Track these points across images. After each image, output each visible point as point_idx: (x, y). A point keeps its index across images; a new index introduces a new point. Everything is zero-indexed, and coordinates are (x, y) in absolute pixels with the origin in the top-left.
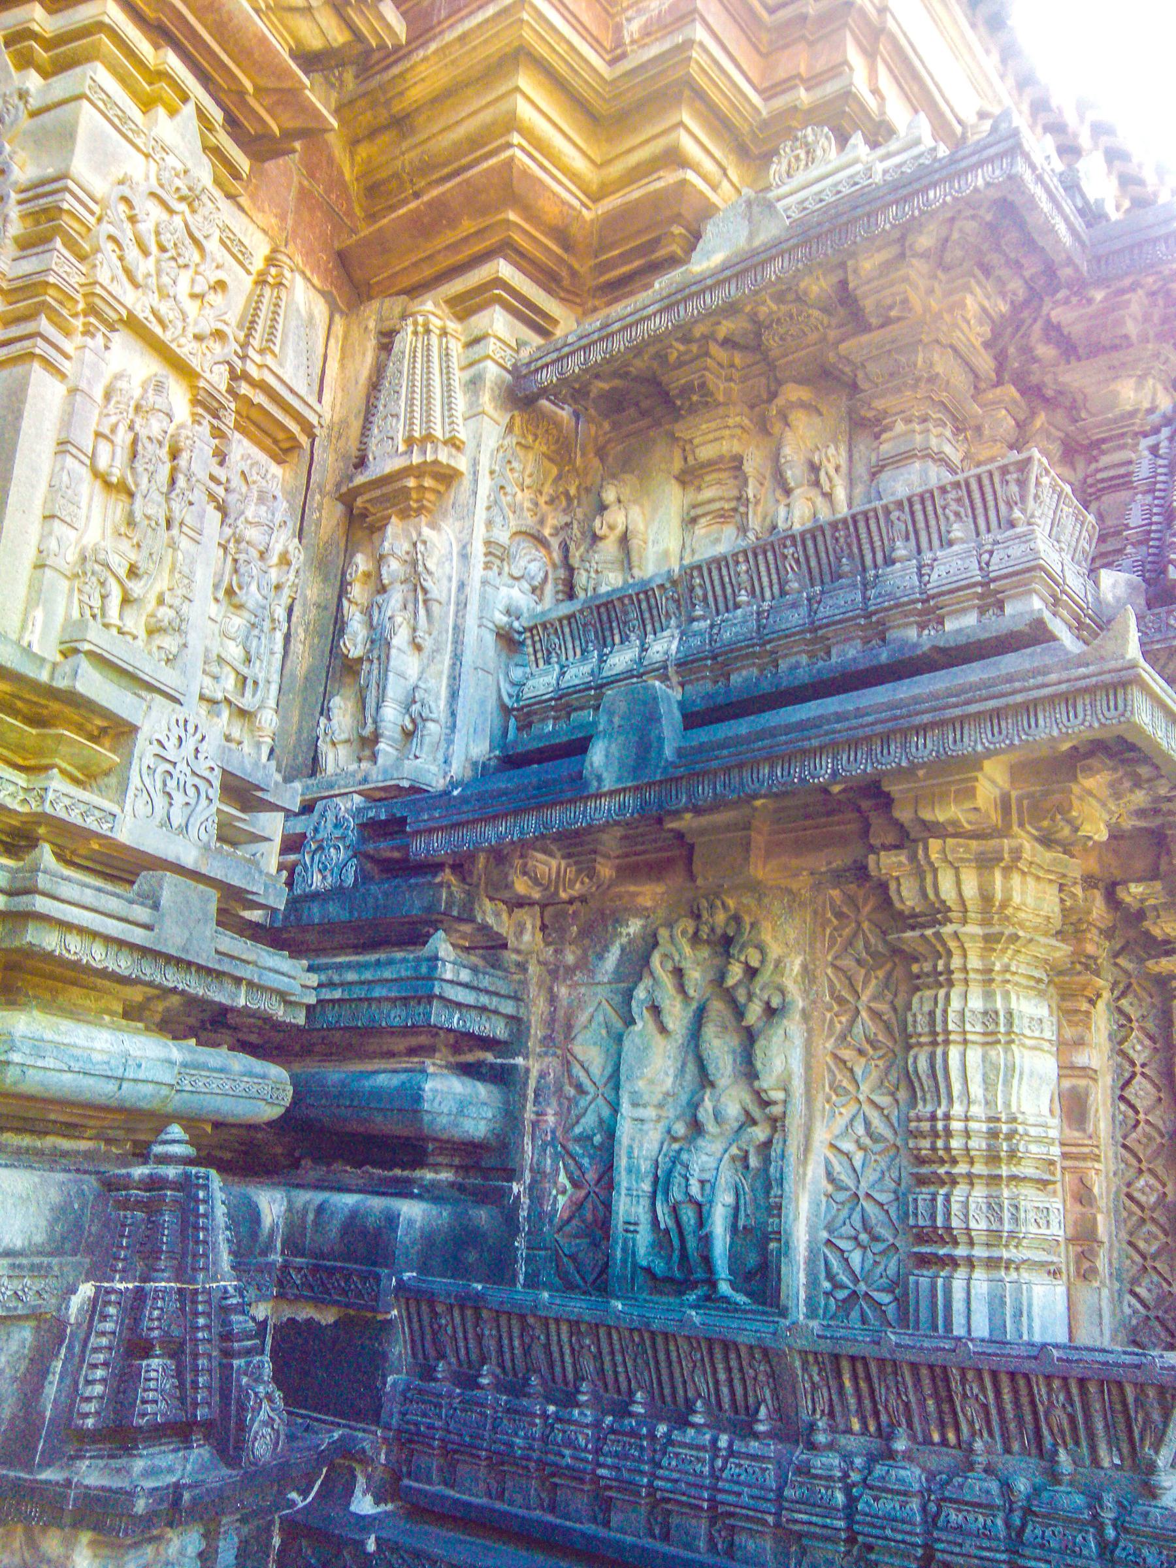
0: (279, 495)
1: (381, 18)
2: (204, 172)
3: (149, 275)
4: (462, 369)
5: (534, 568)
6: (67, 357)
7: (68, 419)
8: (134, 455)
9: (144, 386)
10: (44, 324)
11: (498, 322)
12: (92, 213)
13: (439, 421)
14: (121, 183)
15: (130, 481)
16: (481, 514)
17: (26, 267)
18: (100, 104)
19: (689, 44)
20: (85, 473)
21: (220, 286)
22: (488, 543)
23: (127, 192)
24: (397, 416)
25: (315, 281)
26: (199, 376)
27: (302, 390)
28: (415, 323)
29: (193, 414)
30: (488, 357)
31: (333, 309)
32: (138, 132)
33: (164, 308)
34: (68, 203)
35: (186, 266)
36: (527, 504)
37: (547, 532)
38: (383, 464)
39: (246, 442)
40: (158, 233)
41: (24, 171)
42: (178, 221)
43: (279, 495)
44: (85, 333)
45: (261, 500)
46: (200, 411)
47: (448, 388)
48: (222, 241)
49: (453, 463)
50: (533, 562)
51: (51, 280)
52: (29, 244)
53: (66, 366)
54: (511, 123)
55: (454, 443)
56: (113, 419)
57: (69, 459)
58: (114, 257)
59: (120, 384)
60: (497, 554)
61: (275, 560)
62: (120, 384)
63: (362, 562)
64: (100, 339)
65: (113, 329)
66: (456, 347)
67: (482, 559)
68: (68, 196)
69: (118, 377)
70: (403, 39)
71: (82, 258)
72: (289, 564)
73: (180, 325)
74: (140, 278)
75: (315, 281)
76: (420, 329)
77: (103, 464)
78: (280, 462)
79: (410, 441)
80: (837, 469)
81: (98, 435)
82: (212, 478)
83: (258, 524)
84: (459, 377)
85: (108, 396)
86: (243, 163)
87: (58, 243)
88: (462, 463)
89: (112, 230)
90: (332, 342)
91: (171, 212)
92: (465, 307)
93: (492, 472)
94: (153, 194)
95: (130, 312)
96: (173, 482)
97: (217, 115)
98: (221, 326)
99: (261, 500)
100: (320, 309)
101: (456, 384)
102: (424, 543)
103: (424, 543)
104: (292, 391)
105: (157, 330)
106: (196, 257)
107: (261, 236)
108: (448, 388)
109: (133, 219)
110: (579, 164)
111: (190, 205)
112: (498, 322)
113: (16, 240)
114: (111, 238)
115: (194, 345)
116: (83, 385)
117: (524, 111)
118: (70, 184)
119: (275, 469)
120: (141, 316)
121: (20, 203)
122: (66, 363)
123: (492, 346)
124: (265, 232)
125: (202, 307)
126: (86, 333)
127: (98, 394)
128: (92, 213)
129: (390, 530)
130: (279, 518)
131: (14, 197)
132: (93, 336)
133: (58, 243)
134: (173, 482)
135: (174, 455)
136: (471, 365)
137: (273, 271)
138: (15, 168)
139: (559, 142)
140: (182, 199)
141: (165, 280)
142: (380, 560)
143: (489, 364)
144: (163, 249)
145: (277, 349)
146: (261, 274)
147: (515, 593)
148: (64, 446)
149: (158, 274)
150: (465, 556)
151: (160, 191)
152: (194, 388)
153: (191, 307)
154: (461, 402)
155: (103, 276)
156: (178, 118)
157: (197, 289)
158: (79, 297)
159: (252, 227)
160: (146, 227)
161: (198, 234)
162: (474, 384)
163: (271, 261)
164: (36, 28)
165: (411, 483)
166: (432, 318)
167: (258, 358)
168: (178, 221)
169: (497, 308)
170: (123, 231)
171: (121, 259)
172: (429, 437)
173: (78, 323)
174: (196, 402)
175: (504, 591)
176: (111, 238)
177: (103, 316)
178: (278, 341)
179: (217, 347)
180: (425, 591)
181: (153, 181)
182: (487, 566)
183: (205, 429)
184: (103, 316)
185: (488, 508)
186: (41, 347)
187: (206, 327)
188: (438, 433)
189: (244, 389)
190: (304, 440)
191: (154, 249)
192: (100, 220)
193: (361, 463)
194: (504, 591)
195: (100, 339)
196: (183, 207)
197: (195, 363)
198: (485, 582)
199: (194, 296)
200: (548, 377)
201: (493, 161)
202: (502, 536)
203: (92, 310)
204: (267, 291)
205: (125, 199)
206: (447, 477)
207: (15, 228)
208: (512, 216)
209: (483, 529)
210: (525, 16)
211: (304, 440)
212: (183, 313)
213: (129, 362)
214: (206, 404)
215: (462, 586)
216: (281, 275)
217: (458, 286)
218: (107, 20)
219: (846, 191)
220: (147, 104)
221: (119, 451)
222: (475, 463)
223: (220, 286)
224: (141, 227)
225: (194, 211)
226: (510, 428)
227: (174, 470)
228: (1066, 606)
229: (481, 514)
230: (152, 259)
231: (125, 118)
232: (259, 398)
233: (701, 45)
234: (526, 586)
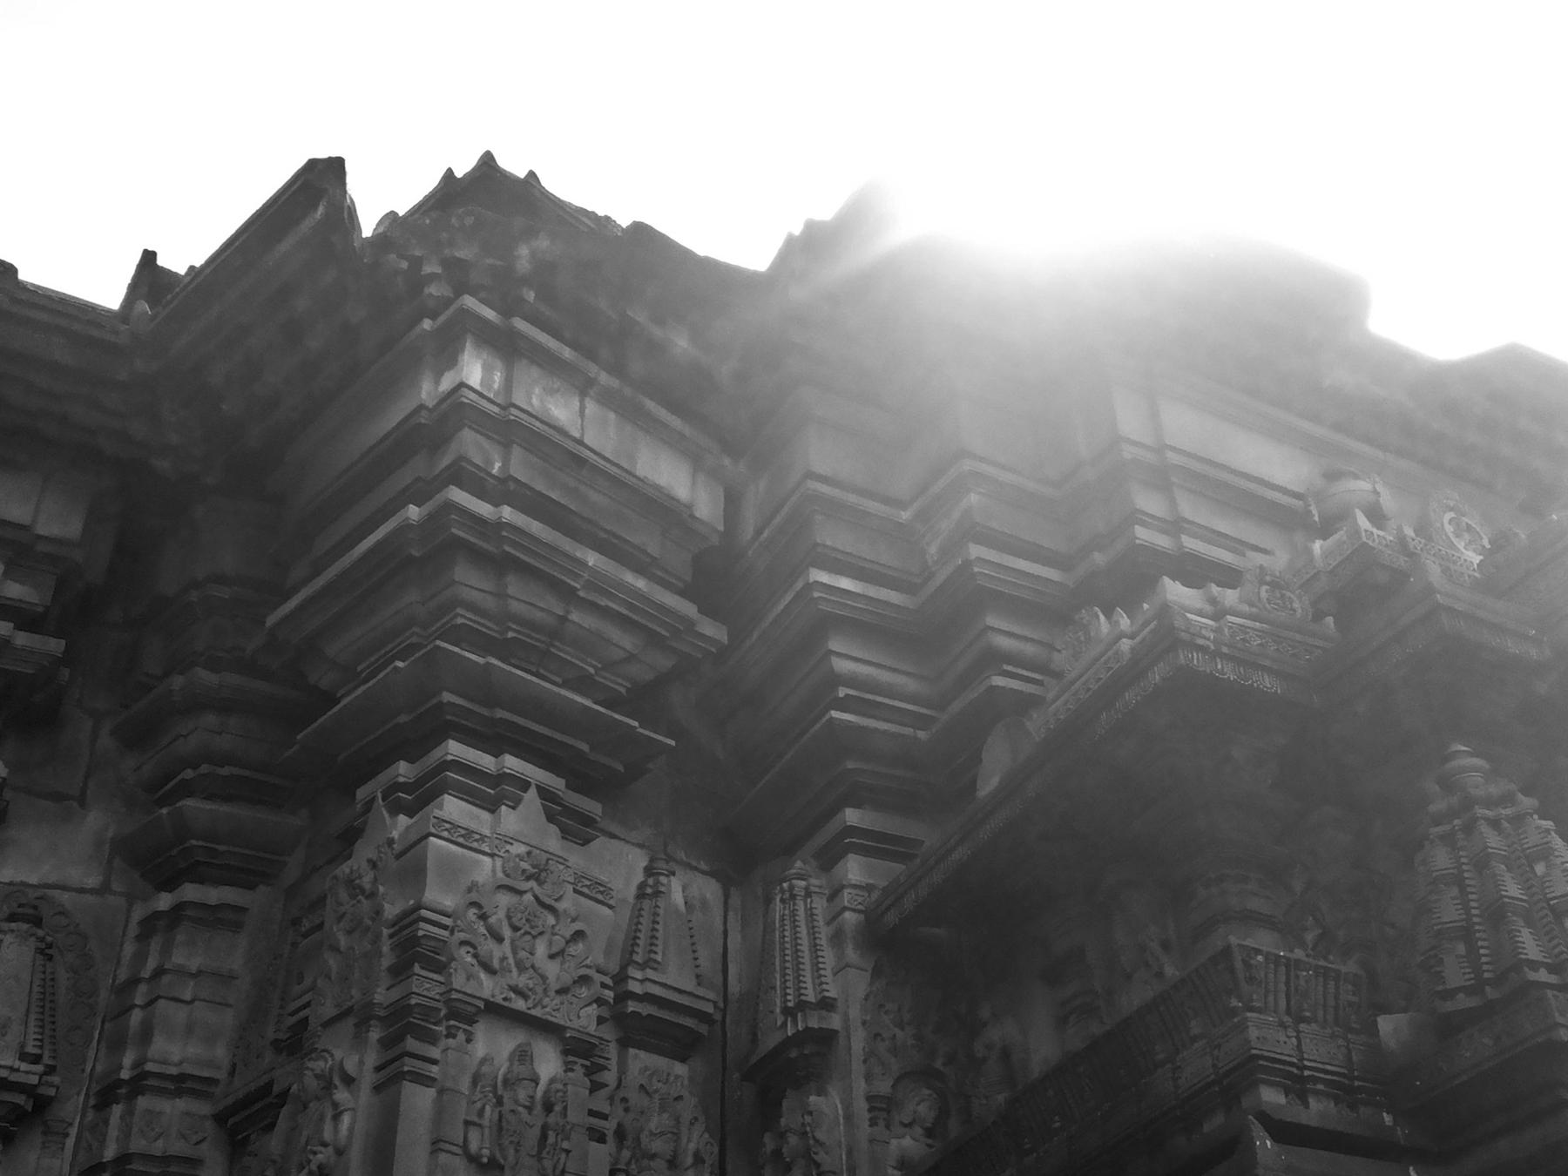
0: (685, 1093)
1: (702, 636)
2: (552, 841)
3: (503, 959)
4: (828, 924)
5: (922, 1109)
6: (435, 1062)
7: (440, 1113)
8: (500, 1129)
9: (511, 1059)
10: (411, 1044)
11: (854, 869)
12: (445, 927)
13: (809, 985)
14: (470, 890)
15: (498, 1156)
16: (857, 1067)
17: (395, 994)
18: (445, 834)
19: (968, 564)
20: (459, 1163)
21: (579, 935)
22: (869, 1098)
23: (474, 897)
24: (774, 988)
25: (703, 866)
26: (565, 1028)
27: (689, 986)
28: (783, 891)
29: (566, 1063)
30: (845, 909)
31: (727, 883)
32: (483, 838)
33: (522, 981)
34: (424, 929)
35: (541, 933)
36: (910, 1042)
37: (938, 1064)
38: (771, 1041)
39: (642, 1054)
40: (509, 918)
41: (391, 910)
42: (528, 897)
43: (685, 1093)
44: (447, 1036)
45: (663, 1109)
46: (571, 1058)
47: (815, 948)
48: (575, 891)
49: (824, 1026)
50: (920, 1105)
51: (413, 1002)
52: (400, 971)
53: (434, 1070)
54: (837, 680)
55: (826, 1004)
56: (479, 1105)
57: (443, 1157)
58: (469, 959)
59: (485, 1069)
60: (882, 1107)
61: (689, 1160)
62: (485, 1069)
63: (769, 1143)
64: (461, 1036)
65: (472, 1022)
66: (819, 904)
67: (867, 1116)
68: (422, 925)
69: (483, 1061)
70: (725, 639)
71: (440, 968)
72: (703, 1162)
73: (539, 990)
74: (496, 964)
75: (703, 866)
76: (787, 895)
77: (474, 1147)
78: (683, 1060)
79: (787, 1011)
80: (1166, 946)
81: (467, 1123)
82: (592, 1113)
83: (662, 1134)
84: (824, 933)
85: (475, 1083)
86: (593, 807)
87: (417, 968)
88: (835, 1022)
89: (462, 936)
90: (731, 914)
91: (521, 893)
92: (829, 859)
93: (864, 1023)
94: (500, 887)
95: (487, 1002)
96: (544, 1137)
97: (556, 783)
98: (583, 971)
99: (663, 1109)
100: (710, 889)
101: (823, 941)
102: (810, 1113)
103: (810, 1113)
104: (680, 991)
105: (520, 1004)
106: (551, 920)
107: (638, 851)
108: (815, 948)
109: (483, 917)
110: (911, 685)
111: (537, 880)
112: (854, 869)
113: (390, 970)
114: (463, 943)
115: (558, 1000)
116: (449, 1084)
117: (842, 666)
118: (424, 913)
119: (680, 1069)
120: (499, 1000)
121: (391, 936)
122: (435, 1069)
123: (847, 896)
124: (640, 846)
125: (562, 963)
126: (450, 1035)
127: (465, 1085)
128: (445, 927)
129: (785, 1103)
130: (687, 1117)
131: (386, 932)
132: (454, 1037)
133: (417, 968)
134: (544, 1137)
135: (548, 1107)
136: (834, 918)
137: (651, 881)
138: (387, 906)
139: (885, 677)
140: (528, 878)
141: (522, 954)
142: (782, 1136)
143: (847, 915)
144: (515, 929)
145: (659, 958)
146: (642, 886)
147: (907, 1142)
148: (437, 1145)
149: (515, 952)
150: (849, 1117)
151: (507, 882)
152: (563, 1040)
153: (552, 969)
154: (828, 958)
155: (458, 981)
156: (521, 807)
157: (555, 950)
158: (439, 1005)
159: (627, 848)
160: (498, 918)
161: (548, 901)
162: (837, 939)
163: (649, 871)
164: (401, 780)
165: (794, 1054)
166: (795, 882)
167: (639, 975)
168: (528, 897)
169: (851, 856)
170: (474, 932)
171: (475, 956)
172: (802, 1006)
173: (441, 1029)
174: (565, 1052)
175: (894, 1142)
176: (463, 943)
177: (465, 1014)
178: (659, 949)
179: (584, 992)
180: (818, 1165)
181: (500, 875)
182: (873, 1122)
183: (579, 1072)
184: (465, 1014)
185: (865, 1061)
186: (409, 1065)
187: (567, 979)
188: (811, 996)
189: (632, 1007)
190: (703, 1029)
191: (507, 933)
192: (452, 933)
193: (754, 1040)
194: (894, 1142)
195: (461, 1036)
196: (532, 884)
197: (559, 1019)
198: (872, 1141)
199: (552, 957)
200: (891, 918)
201: (818, 726)
202: (884, 1087)
203: (454, 1014)
204: (647, 904)
205: (474, 904)
206: (826, 1038)
207: (386, 962)
208: (850, 765)
209: (863, 1083)
210: (816, 595)
211: (703, 1029)
212: (544, 978)
213: (492, 1046)
214: (577, 1049)
215: (850, 1153)
216: (658, 883)
217: (820, 839)
218: (450, 758)
219: (1094, 687)
220: (492, 806)
221: (487, 1131)
222: (846, 1019)
223: (579, 935)
224: (492, 920)
225: (541, 883)
226: (877, 972)
227: (545, 1129)
228: (1316, 1080)
229: (857, 1067)
230: (507, 942)
231: (469, 833)
232: (645, 1009)
233: (979, 559)
234: (918, 1130)
